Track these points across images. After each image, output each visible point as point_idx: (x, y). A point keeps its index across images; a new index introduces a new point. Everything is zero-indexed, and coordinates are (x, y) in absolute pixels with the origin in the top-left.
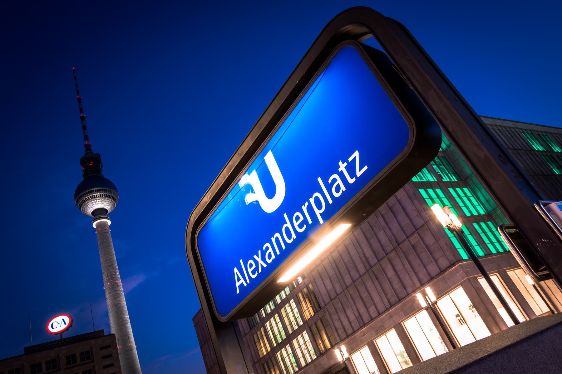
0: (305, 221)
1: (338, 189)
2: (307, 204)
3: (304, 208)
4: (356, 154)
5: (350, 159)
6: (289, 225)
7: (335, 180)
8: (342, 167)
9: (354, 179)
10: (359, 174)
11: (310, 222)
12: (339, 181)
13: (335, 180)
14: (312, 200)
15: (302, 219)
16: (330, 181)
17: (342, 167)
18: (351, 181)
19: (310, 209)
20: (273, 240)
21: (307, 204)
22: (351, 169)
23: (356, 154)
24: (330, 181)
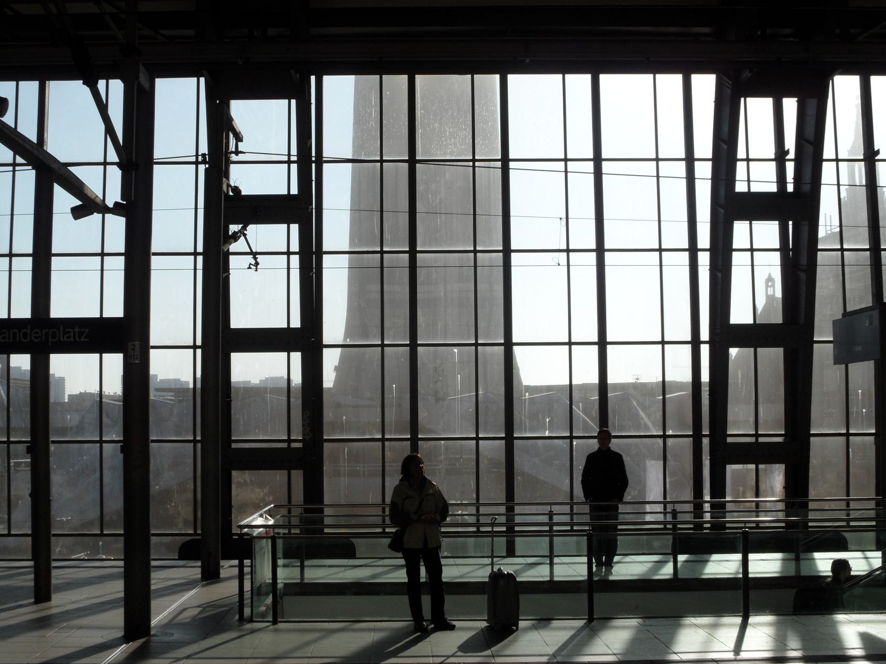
1: (69, 337)
2: (47, 330)
3: (44, 332)
4: (87, 330)
6: (29, 332)
7: (69, 332)
8: (77, 330)
9: (78, 340)
11: (44, 340)
13: (69, 332)
14: (50, 332)
15: (40, 335)
16: (67, 330)
17: (77, 330)
18: (78, 340)
20: (12, 331)
21: (47, 330)
22: (81, 334)
23: (87, 330)
24: (67, 330)
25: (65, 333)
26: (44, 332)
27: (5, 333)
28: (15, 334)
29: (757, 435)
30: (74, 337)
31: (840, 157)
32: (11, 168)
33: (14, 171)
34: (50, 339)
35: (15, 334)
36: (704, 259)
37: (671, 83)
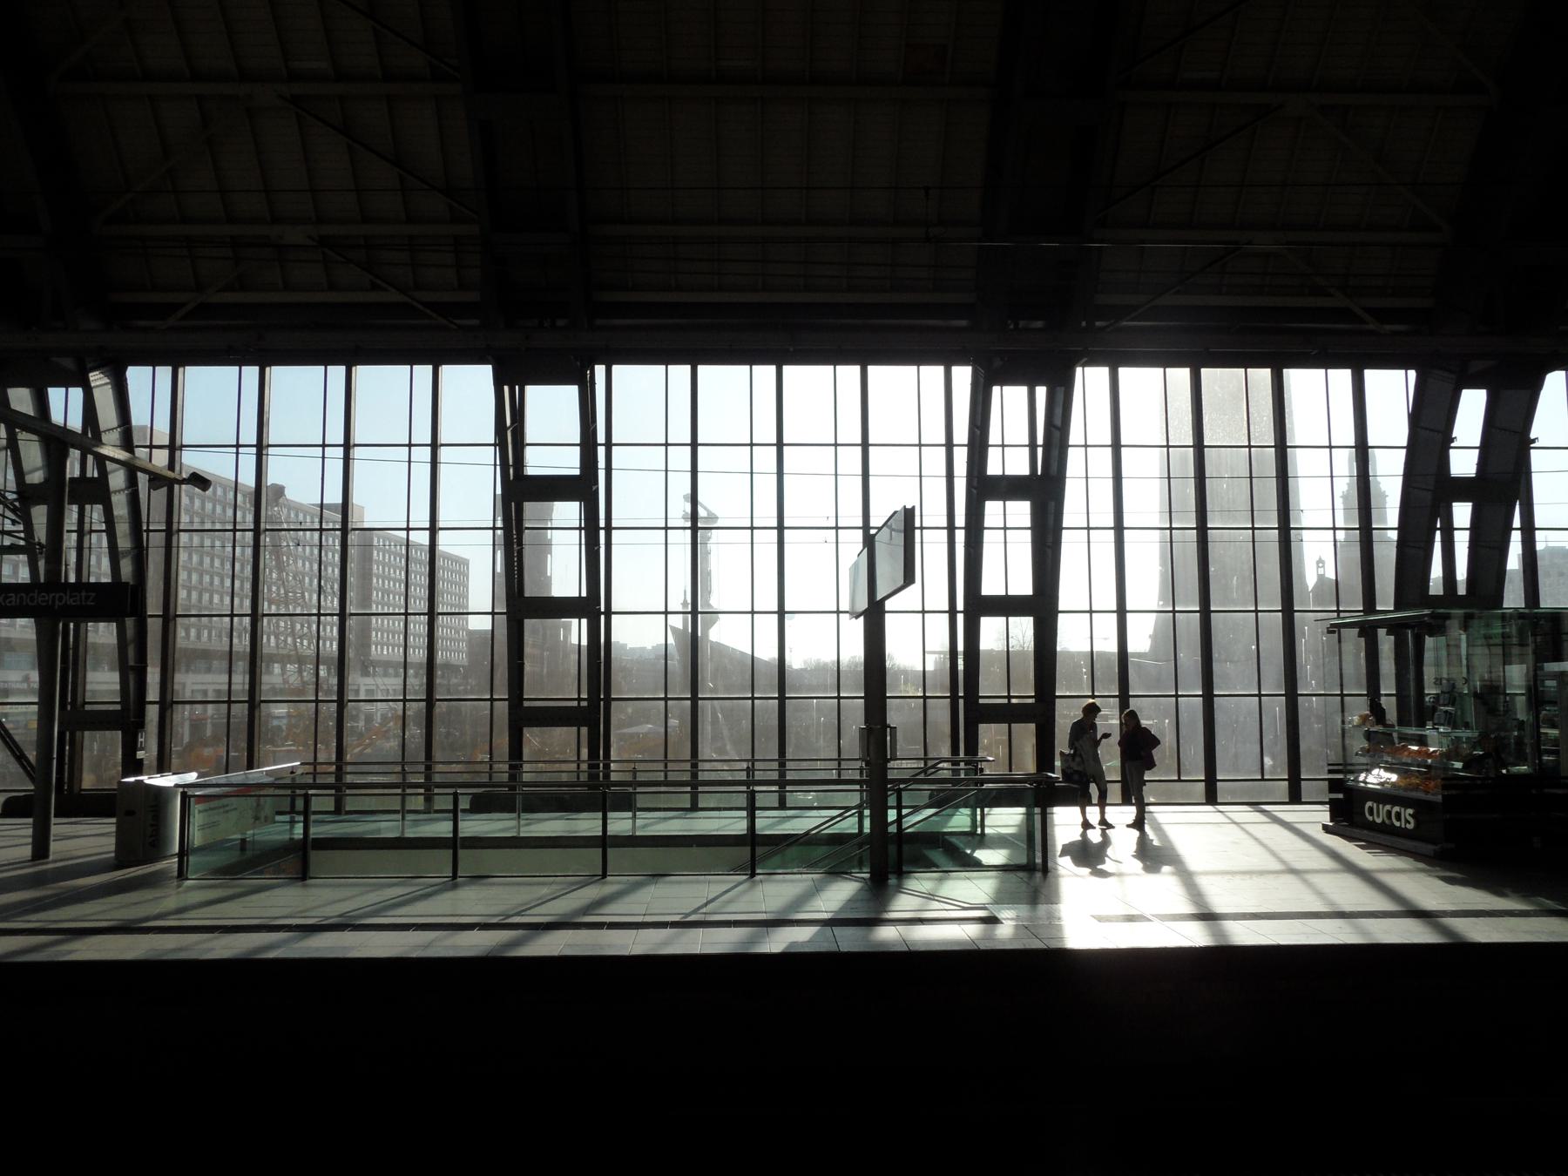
0: (48, 601)
5: (90, 594)
6: (36, 595)
7: (76, 596)
8: (83, 594)
10: (88, 603)
12: (78, 598)
13: (76, 596)
14: (57, 595)
15: (47, 598)
16: (74, 594)
18: (83, 603)
19: (54, 597)
20: (19, 596)
21: (53, 594)
22: (87, 598)
23: (94, 594)
25: (71, 597)
26: (51, 595)
27: (11, 597)
28: (21, 598)
29: (1009, 697)
30: (81, 601)
31: (1088, 444)
32: (234, 450)
33: (237, 453)
34: (57, 602)
35: (21, 597)
36: (960, 536)
37: (933, 374)
